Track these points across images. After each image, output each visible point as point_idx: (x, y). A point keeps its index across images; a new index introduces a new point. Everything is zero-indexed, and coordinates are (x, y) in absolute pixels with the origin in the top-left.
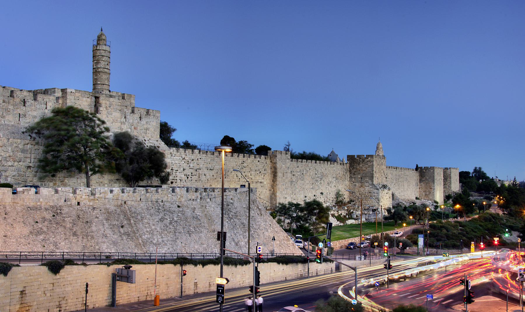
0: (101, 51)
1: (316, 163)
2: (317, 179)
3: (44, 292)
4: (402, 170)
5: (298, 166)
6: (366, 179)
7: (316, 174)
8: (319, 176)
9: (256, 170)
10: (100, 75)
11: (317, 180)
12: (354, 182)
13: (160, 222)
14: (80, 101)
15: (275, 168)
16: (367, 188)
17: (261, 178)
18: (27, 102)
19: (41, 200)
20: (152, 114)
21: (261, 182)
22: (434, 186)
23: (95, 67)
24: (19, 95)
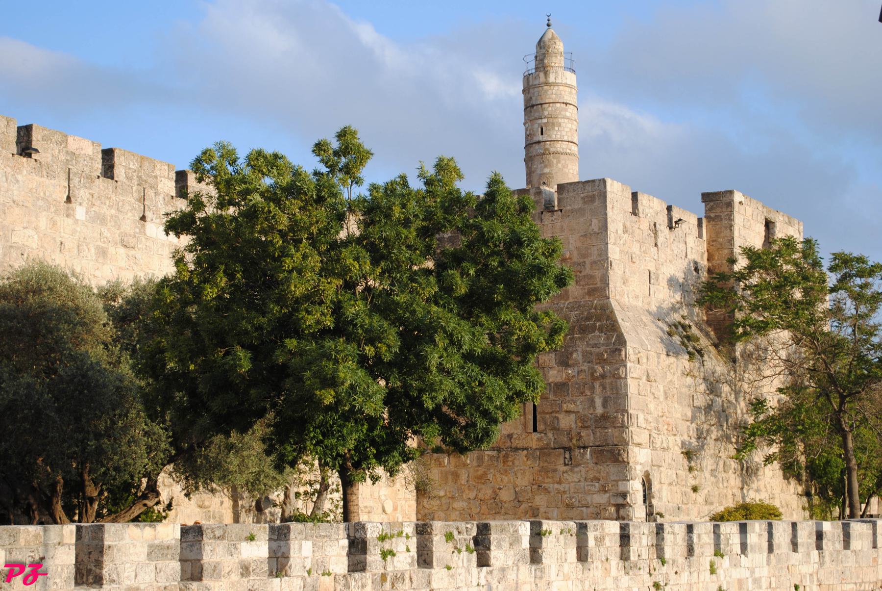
0: (561, 88)
10: (559, 162)
23: (540, 138)
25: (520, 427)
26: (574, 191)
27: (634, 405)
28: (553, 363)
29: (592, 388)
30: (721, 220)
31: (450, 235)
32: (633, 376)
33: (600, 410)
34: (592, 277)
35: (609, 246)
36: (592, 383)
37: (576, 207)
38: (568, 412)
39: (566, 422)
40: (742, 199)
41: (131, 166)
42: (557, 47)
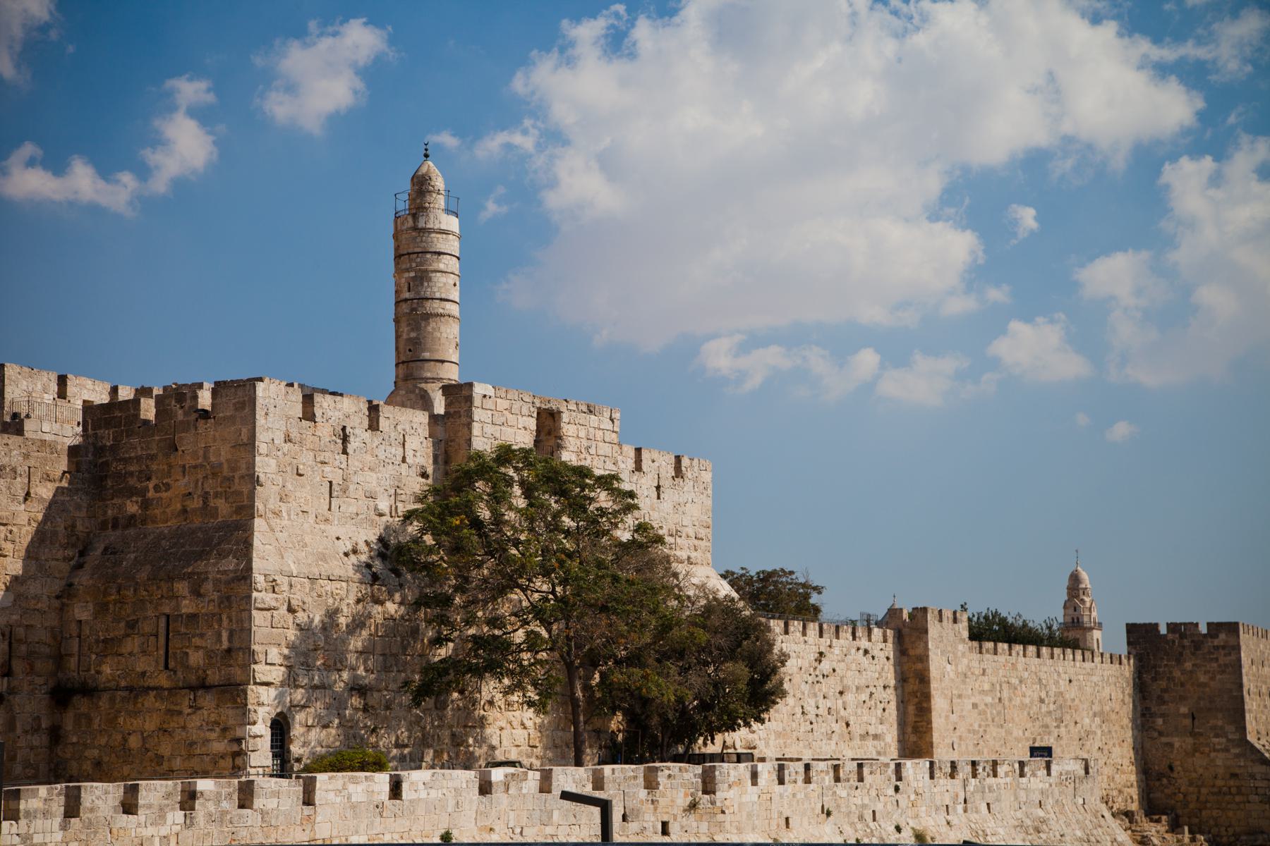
0: (433, 235)
5: (984, 670)
6: (1212, 722)
7: (1042, 701)
8: (1052, 707)
9: (857, 688)
11: (1047, 726)
12: (1161, 734)
14: (509, 429)
15: (924, 678)
16: (1220, 759)
17: (874, 720)
18: (352, 439)
20: (689, 474)
21: (876, 737)
23: (407, 295)
24: (330, 413)
25: (153, 663)
26: (227, 396)
28: (186, 592)
29: (221, 619)
30: (460, 417)
31: (112, 443)
32: (260, 606)
33: (225, 645)
34: (240, 493)
35: (257, 459)
36: (220, 615)
37: (228, 414)
38: (198, 648)
39: (196, 658)
40: (489, 390)
42: (432, 183)
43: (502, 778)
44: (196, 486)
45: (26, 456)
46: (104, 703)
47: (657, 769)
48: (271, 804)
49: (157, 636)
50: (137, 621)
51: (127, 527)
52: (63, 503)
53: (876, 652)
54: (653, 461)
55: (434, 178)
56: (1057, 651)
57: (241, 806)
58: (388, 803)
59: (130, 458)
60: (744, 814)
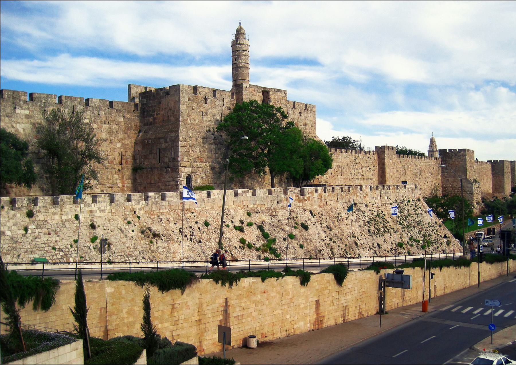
1: (415, 158)
2: (417, 174)
3: (332, 301)
4: (482, 164)
5: (400, 162)
7: (416, 169)
8: (418, 171)
9: (366, 167)
10: (241, 70)
11: (417, 176)
12: (446, 177)
13: (356, 223)
14: (254, 96)
15: (384, 164)
18: (208, 99)
19: (257, 202)
20: (309, 109)
21: (371, 179)
22: (504, 180)
23: (235, 62)
27: (181, 154)
28: (163, 142)
33: (173, 156)
34: (176, 115)
38: (166, 157)
39: (166, 160)
41: (10, 93)
43: (241, 192)
44: (166, 114)
45: (123, 107)
46: (145, 172)
47: (287, 189)
48: (171, 199)
49: (157, 154)
50: (152, 150)
51: (150, 125)
52: (134, 119)
53: (371, 158)
54: (298, 105)
55: (242, 30)
56: (420, 157)
57: (163, 200)
58: (207, 199)
59: (150, 106)
60: (313, 201)
